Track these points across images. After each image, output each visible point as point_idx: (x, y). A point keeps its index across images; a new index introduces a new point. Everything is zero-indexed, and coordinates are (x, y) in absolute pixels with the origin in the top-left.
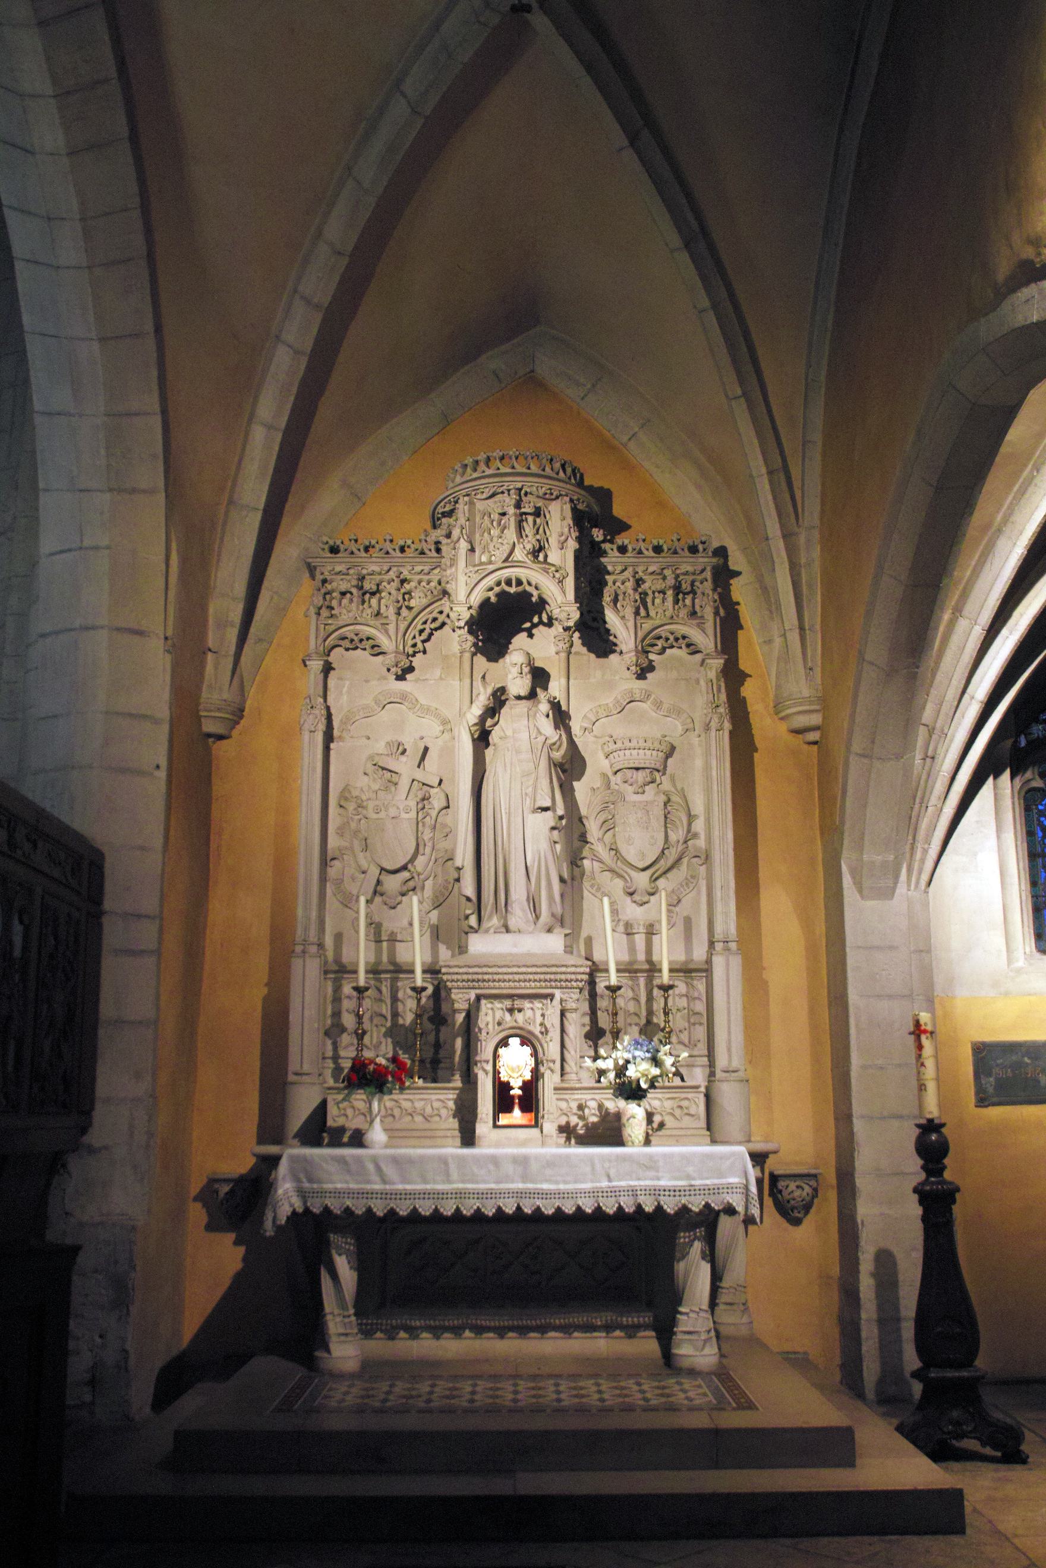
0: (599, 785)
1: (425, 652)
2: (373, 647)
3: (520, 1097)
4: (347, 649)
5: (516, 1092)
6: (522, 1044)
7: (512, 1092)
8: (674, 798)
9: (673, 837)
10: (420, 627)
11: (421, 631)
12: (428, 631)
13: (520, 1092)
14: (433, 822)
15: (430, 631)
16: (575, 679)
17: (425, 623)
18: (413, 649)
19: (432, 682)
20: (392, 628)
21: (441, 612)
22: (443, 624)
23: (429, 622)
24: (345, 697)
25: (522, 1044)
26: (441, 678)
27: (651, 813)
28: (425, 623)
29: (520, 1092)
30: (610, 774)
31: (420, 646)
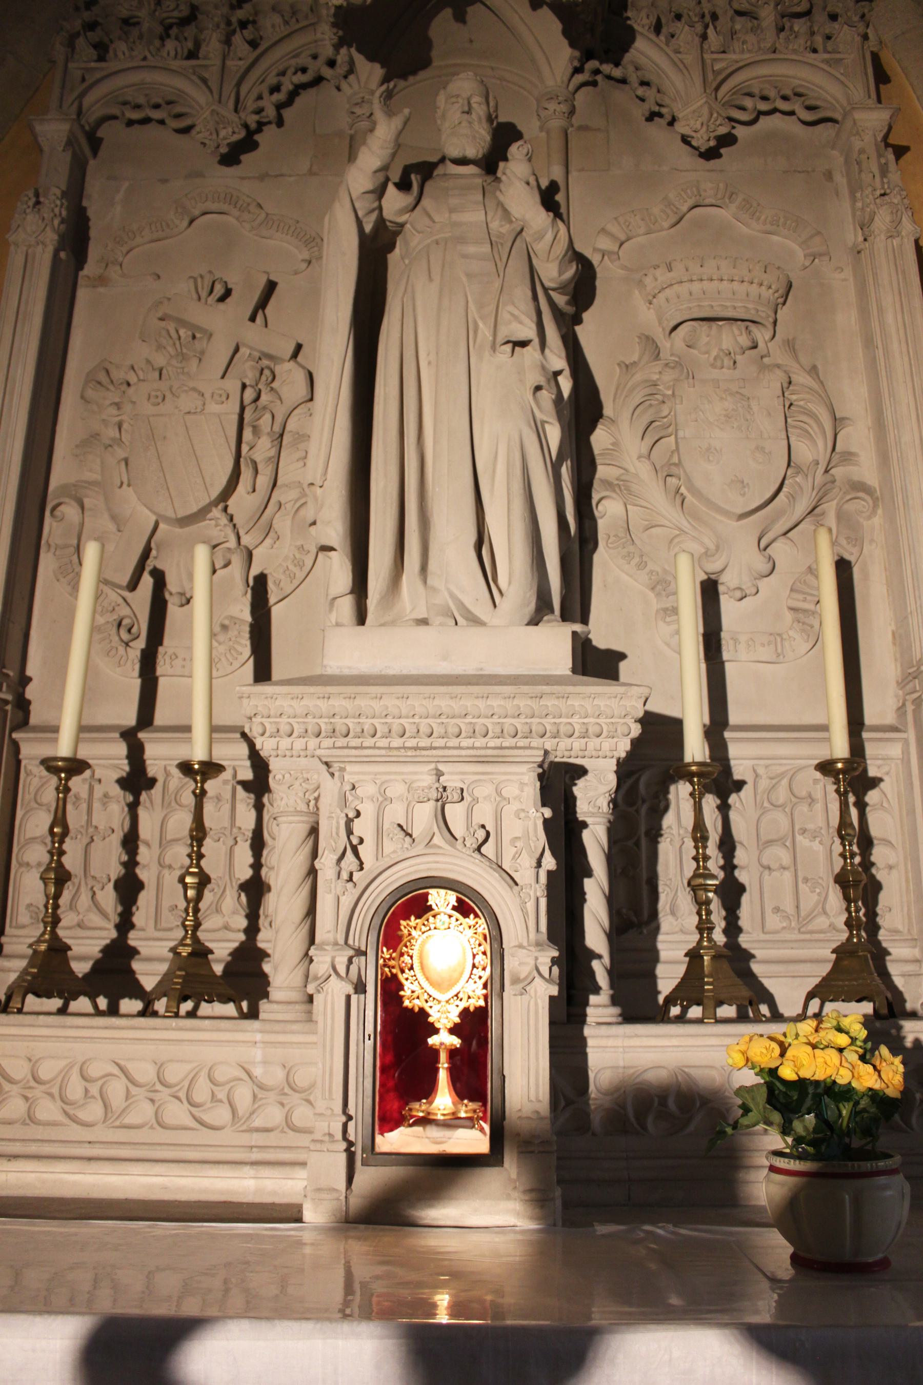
0: (635, 358)
1: (280, 123)
2: (178, 116)
3: (453, 1053)
4: (130, 123)
5: (444, 1040)
6: (463, 908)
7: (433, 1041)
8: (801, 378)
9: (804, 452)
10: (272, 80)
11: (275, 89)
12: (287, 86)
13: (455, 1041)
14: (277, 428)
15: (291, 87)
16: (582, 170)
17: (283, 73)
18: (256, 118)
19: (292, 179)
20: (213, 75)
21: (315, 57)
22: (318, 80)
23: (289, 73)
24: (118, 209)
25: (463, 908)
26: (311, 173)
27: (754, 404)
28: (283, 73)
29: (455, 1041)
30: (659, 335)
31: (271, 112)
